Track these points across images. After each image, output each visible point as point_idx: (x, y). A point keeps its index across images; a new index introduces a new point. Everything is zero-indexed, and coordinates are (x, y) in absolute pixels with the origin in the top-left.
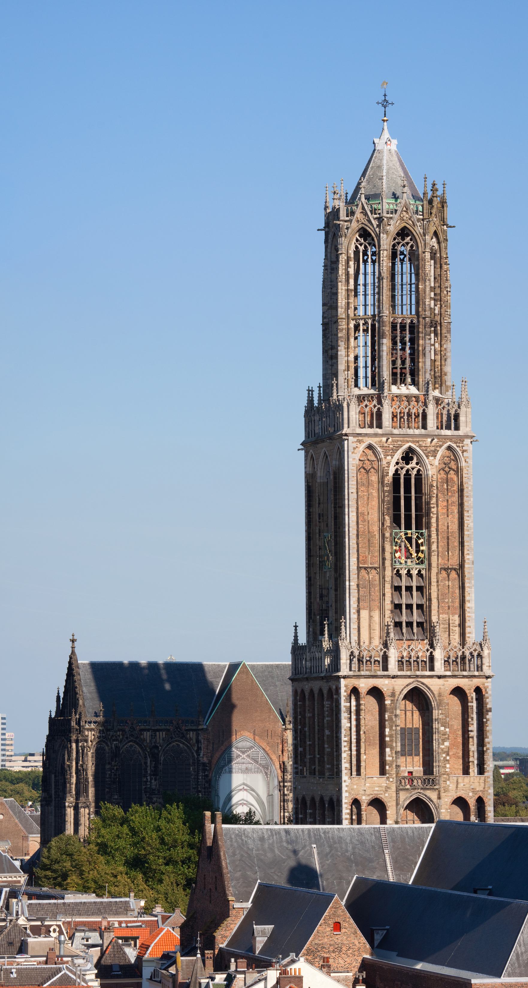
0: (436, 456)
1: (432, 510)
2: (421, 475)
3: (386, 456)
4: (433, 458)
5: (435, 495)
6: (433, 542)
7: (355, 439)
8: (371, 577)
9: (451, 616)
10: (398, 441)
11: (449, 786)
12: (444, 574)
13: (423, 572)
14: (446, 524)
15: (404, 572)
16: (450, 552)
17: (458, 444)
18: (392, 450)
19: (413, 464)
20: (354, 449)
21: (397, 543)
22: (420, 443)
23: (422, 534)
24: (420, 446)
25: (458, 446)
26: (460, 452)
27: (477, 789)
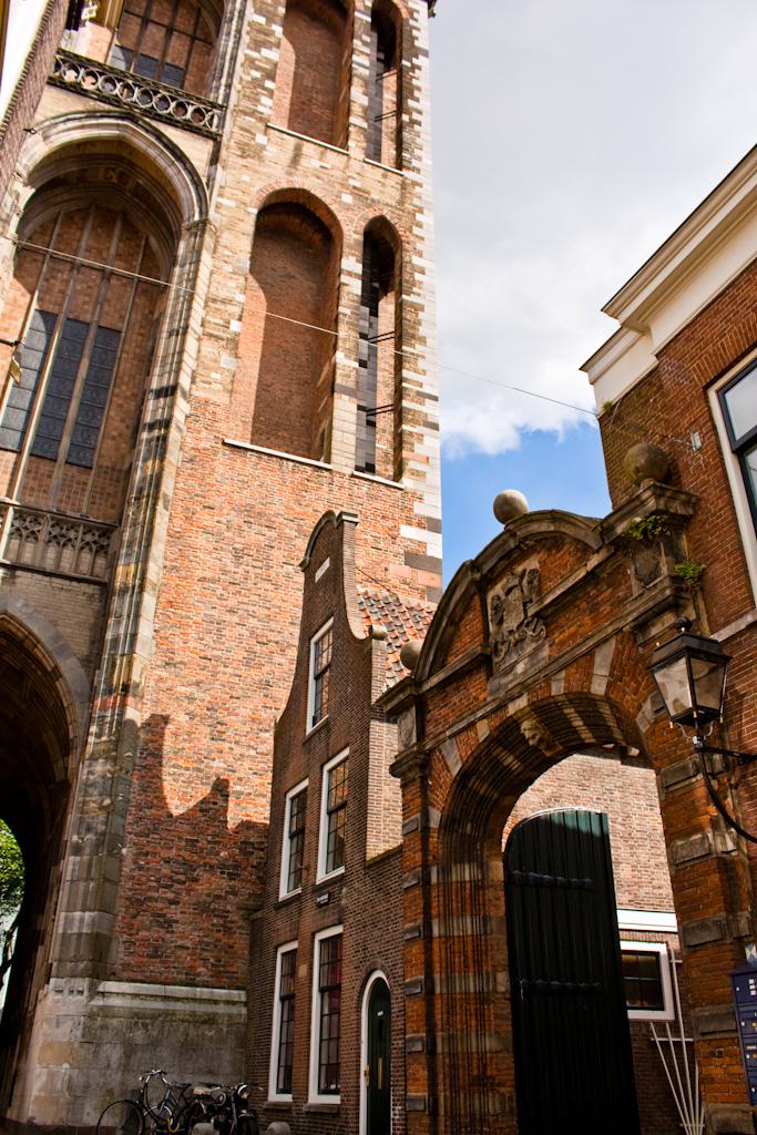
11: (263, 148)
27: (375, 196)
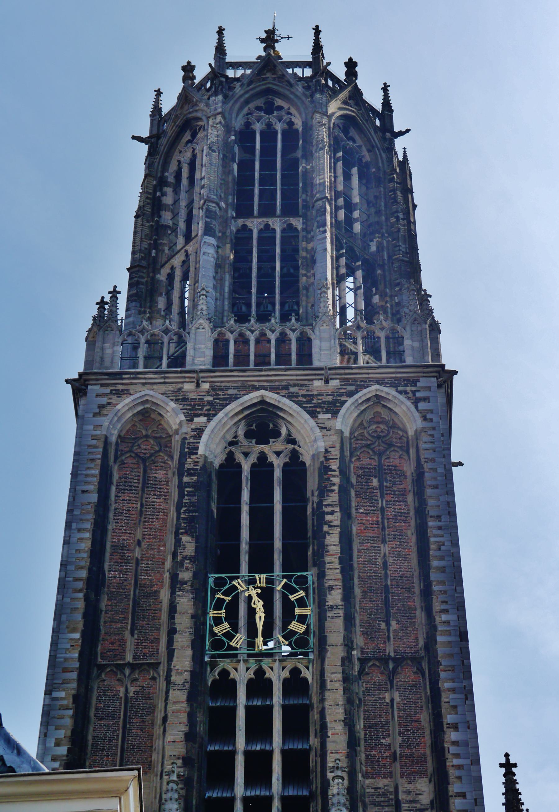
0: (337, 412)
1: (328, 518)
2: (304, 464)
3: (190, 417)
4: (329, 416)
5: (336, 488)
6: (331, 588)
7: (107, 390)
8: (132, 690)
9: (404, 785)
10: (228, 388)
12: (378, 677)
13: (307, 674)
14: (380, 560)
15: (242, 675)
16: (393, 623)
17: (400, 388)
18: (211, 404)
19: (279, 445)
20: (101, 407)
21: (221, 601)
22: (292, 390)
23: (302, 582)
24: (291, 397)
25: (400, 392)
26: (409, 403)
